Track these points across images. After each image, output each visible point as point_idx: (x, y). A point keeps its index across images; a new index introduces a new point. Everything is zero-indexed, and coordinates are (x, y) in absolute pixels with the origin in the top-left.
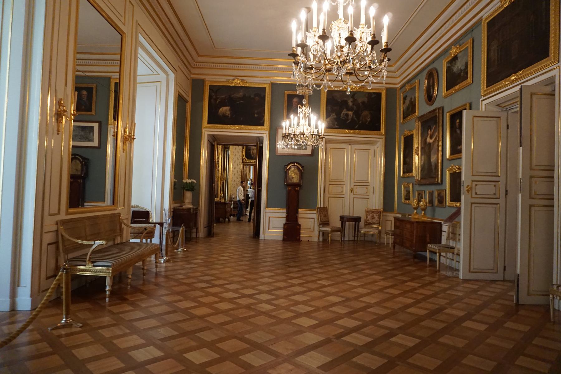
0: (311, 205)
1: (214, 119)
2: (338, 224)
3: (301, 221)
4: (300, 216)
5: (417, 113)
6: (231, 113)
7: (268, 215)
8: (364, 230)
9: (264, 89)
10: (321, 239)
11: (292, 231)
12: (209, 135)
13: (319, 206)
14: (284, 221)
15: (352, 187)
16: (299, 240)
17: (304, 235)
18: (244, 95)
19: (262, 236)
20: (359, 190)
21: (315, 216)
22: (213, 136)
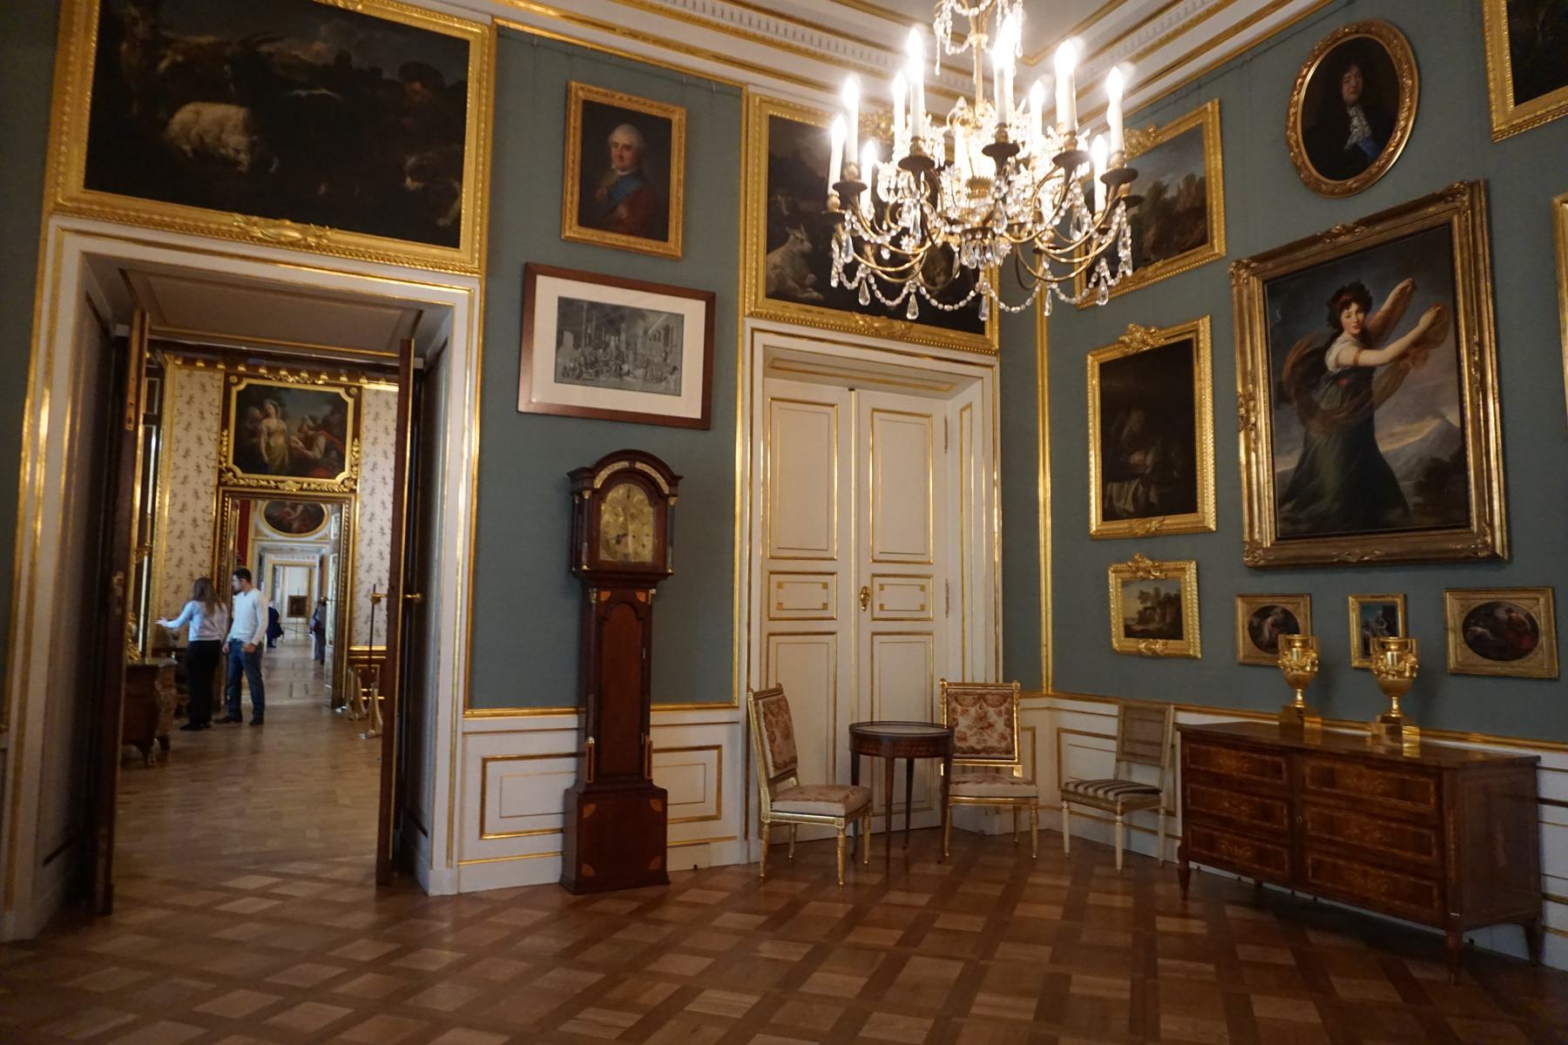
0: (710, 689)
1: (132, 161)
3: (663, 772)
4: (657, 738)
5: (1219, 246)
6: (252, 147)
9: (459, 47)
11: (615, 824)
12: (90, 259)
14: (563, 776)
16: (661, 877)
18: (343, 59)
20: (894, 597)
22: (125, 271)
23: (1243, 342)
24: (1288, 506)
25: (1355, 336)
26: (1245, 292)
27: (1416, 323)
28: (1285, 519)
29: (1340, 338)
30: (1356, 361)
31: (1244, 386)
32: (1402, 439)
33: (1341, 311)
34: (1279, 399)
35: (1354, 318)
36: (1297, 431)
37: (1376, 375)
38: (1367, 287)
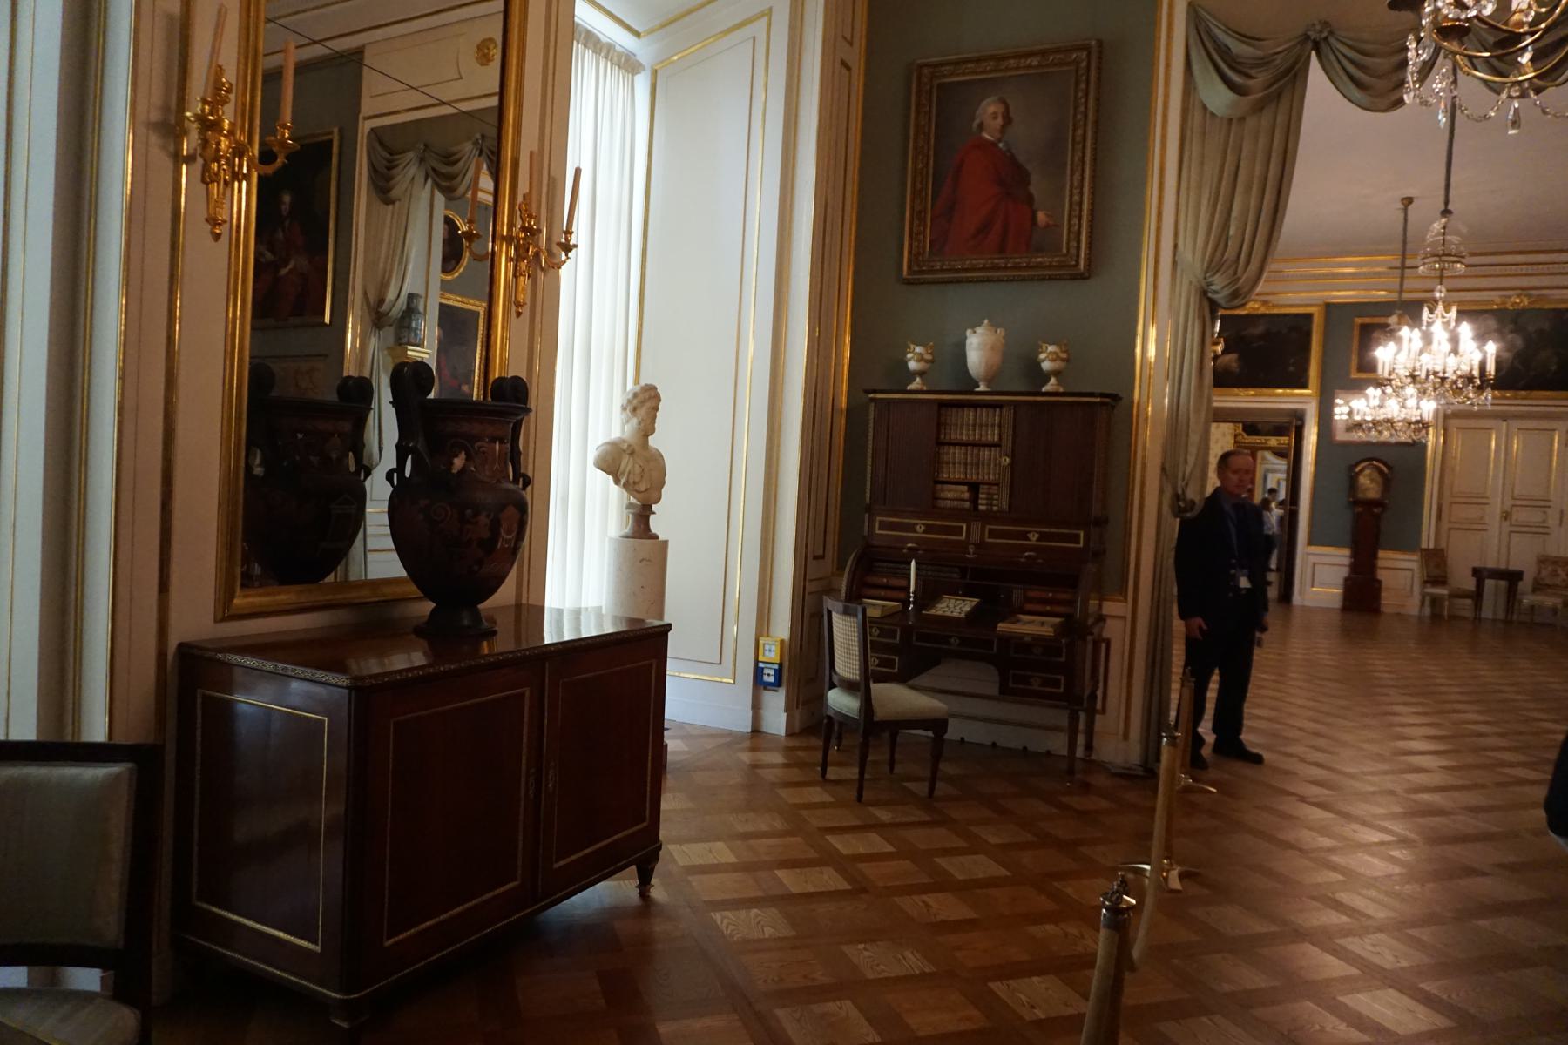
0: (1407, 543)
2: (1470, 584)
3: (1382, 575)
4: (1380, 563)
7: (1312, 559)
8: (1527, 600)
9: (1308, 317)
10: (1427, 611)
11: (1362, 593)
13: (1424, 545)
14: (1344, 572)
15: (1507, 508)
17: (1388, 601)
19: (1297, 599)
21: (1415, 566)
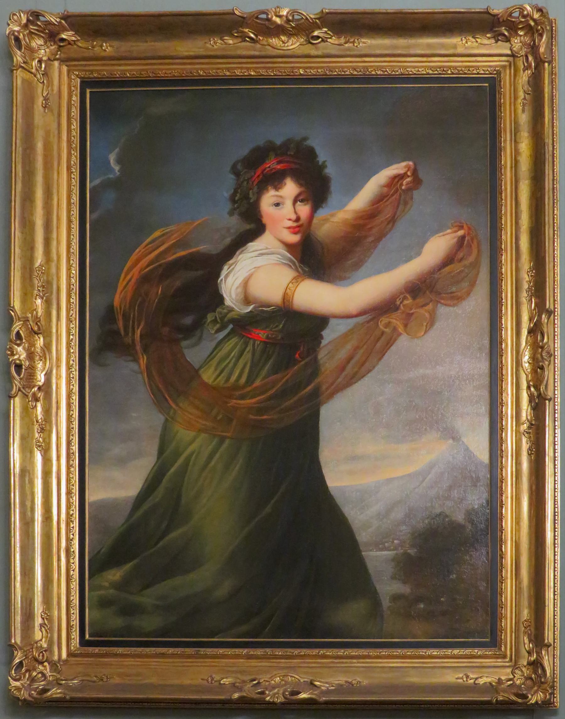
23: (28, 198)
24: (115, 575)
25: (289, 247)
26: (40, 92)
27: (416, 249)
28: (104, 603)
29: (254, 246)
30: (286, 298)
31: (26, 296)
32: (381, 464)
33: (262, 188)
34: (104, 340)
35: (287, 210)
36: (145, 419)
37: (329, 335)
38: (322, 157)
